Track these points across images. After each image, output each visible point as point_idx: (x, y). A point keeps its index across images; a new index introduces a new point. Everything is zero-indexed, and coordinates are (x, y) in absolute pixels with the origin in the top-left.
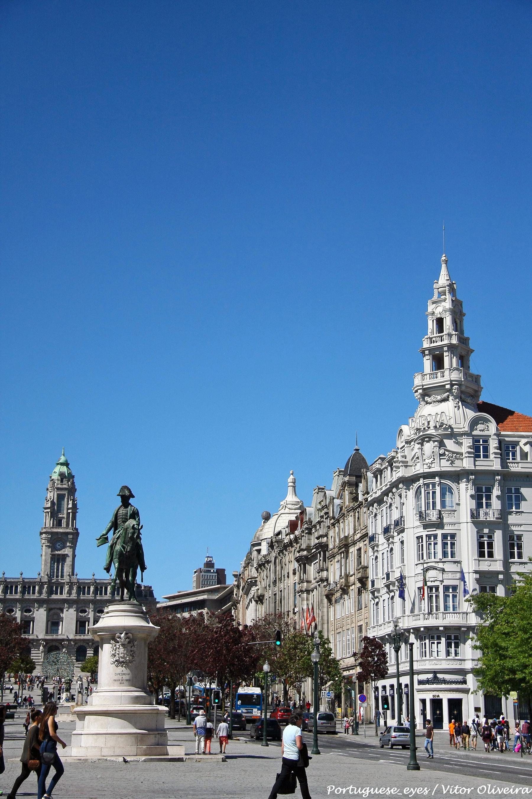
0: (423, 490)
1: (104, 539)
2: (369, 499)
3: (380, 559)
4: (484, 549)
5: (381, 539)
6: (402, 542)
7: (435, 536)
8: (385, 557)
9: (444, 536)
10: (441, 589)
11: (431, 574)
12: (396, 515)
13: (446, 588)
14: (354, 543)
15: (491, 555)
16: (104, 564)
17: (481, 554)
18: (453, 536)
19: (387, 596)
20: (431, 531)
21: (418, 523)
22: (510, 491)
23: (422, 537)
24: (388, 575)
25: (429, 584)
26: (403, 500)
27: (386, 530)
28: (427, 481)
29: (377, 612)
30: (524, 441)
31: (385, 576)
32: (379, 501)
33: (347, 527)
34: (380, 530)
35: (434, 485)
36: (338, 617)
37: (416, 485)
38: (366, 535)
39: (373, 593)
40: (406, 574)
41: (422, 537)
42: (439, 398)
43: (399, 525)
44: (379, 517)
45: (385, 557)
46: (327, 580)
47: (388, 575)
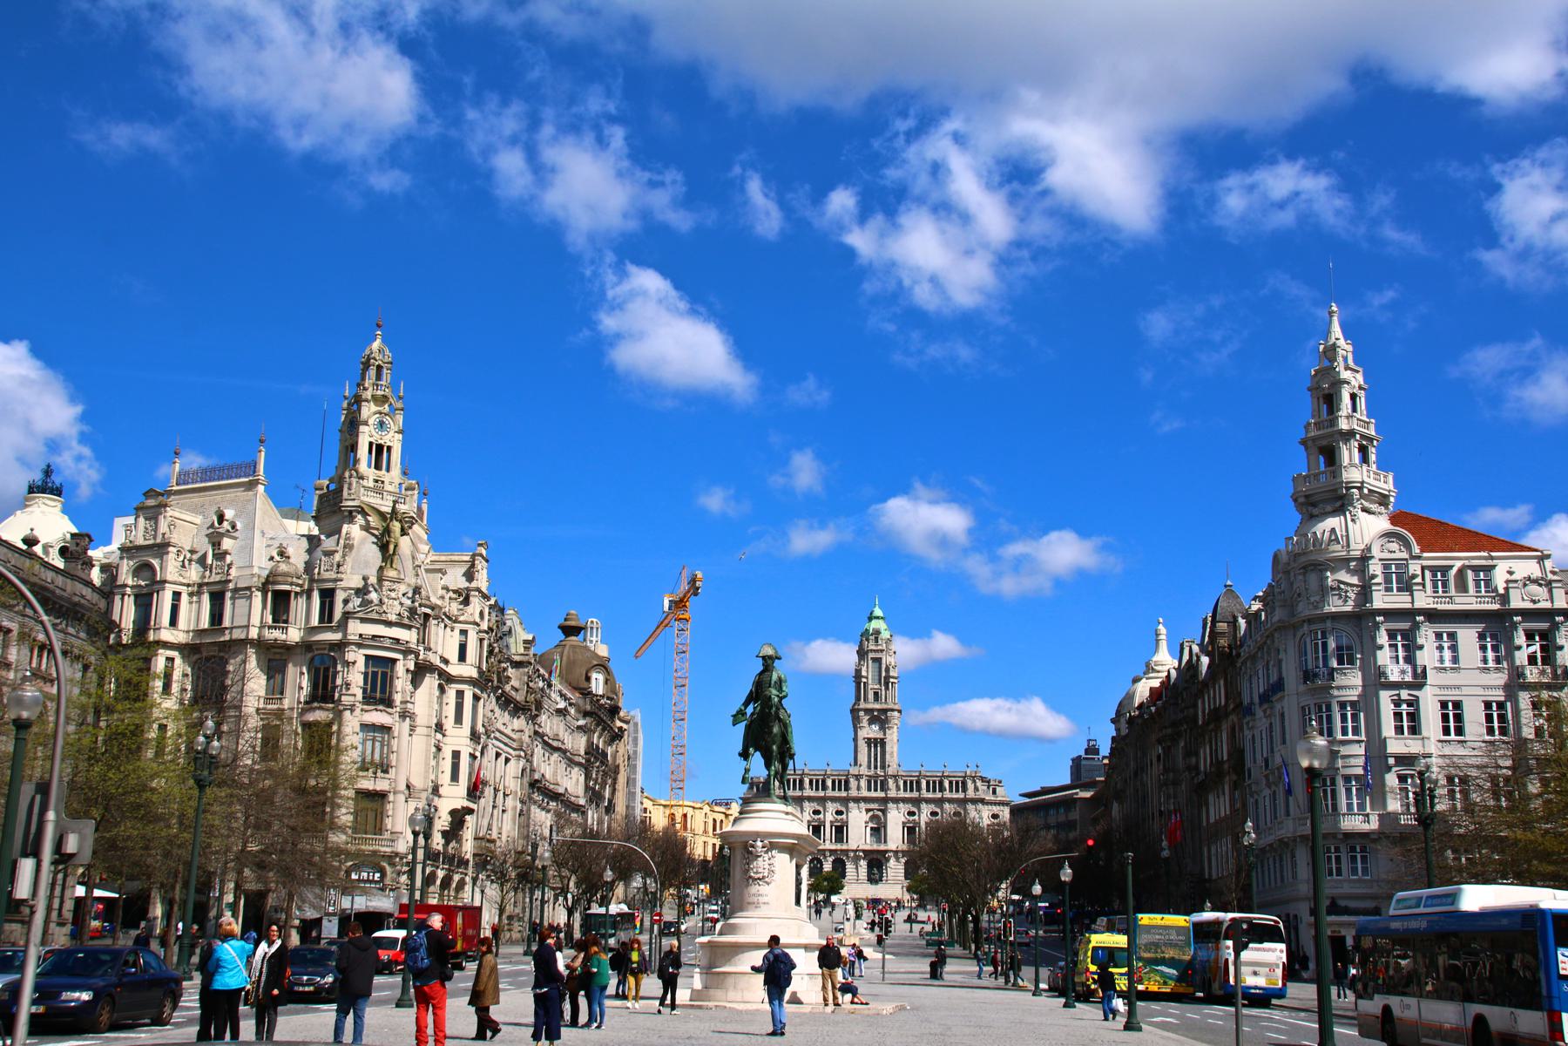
1: (737, 717)
6: (1282, 715)
9: (1343, 705)
12: (1274, 678)
13: (1347, 779)
14: (1227, 715)
15: (1415, 730)
16: (740, 748)
19: (1267, 792)
27: (1265, 698)
28: (1313, 627)
30: (1458, 564)
32: (1253, 658)
33: (1219, 695)
34: (1256, 700)
36: (1212, 820)
37: (1299, 634)
42: (1329, 508)
44: (1254, 680)
46: (1197, 767)
47: (1266, 761)
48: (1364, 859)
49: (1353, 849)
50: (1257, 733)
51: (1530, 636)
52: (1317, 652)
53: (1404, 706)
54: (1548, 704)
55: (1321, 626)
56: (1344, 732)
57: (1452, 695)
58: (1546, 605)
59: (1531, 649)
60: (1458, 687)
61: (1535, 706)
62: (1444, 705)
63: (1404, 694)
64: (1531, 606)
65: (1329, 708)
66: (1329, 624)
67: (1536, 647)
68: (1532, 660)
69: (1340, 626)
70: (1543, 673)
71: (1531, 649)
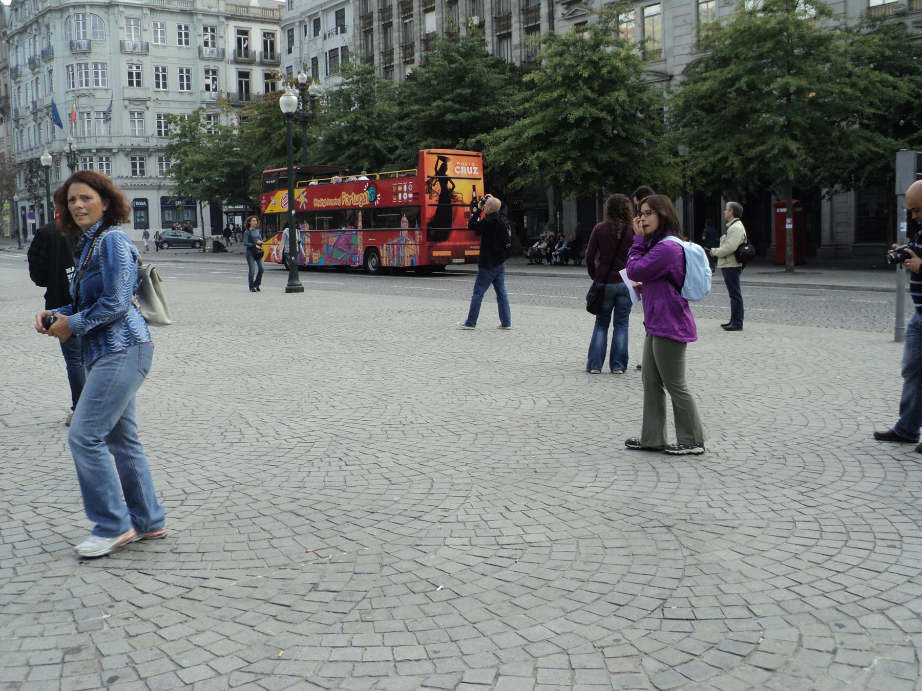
0: (73, 20)
2: (8, 32)
3: (23, 90)
4: (134, 79)
5: (26, 71)
6: (50, 72)
7: (86, 65)
8: (29, 86)
9: (96, 65)
10: (92, 115)
11: (83, 101)
13: (98, 113)
15: (139, 84)
17: (131, 83)
18: (103, 64)
19: (34, 123)
20: (82, 59)
21: (68, 52)
22: (155, 25)
23: (72, 65)
24: (34, 103)
25: (82, 110)
26: (52, 30)
28: (77, 11)
29: (22, 139)
31: (30, 104)
35: (84, 16)
37: (65, 16)
38: (6, 67)
39: (17, 121)
40: (57, 102)
41: (72, 65)
43: (47, 54)
45: (29, 86)
48: (108, 165)
49: (101, 159)
50: (22, 85)
51: (206, 29)
52: (78, 28)
53: (134, 68)
54: (214, 72)
55: (82, 11)
56: (97, 83)
57: (160, 65)
58: (214, 10)
59: (206, 37)
60: (165, 58)
61: (207, 72)
62: (157, 69)
63: (135, 60)
64: (207, 9)
65: (86, 68)
66: (88, 10)
67: (209, 36)
68: (206, 44)
69: (96, 11)
70: (212, 52)
71: (206, 37)
